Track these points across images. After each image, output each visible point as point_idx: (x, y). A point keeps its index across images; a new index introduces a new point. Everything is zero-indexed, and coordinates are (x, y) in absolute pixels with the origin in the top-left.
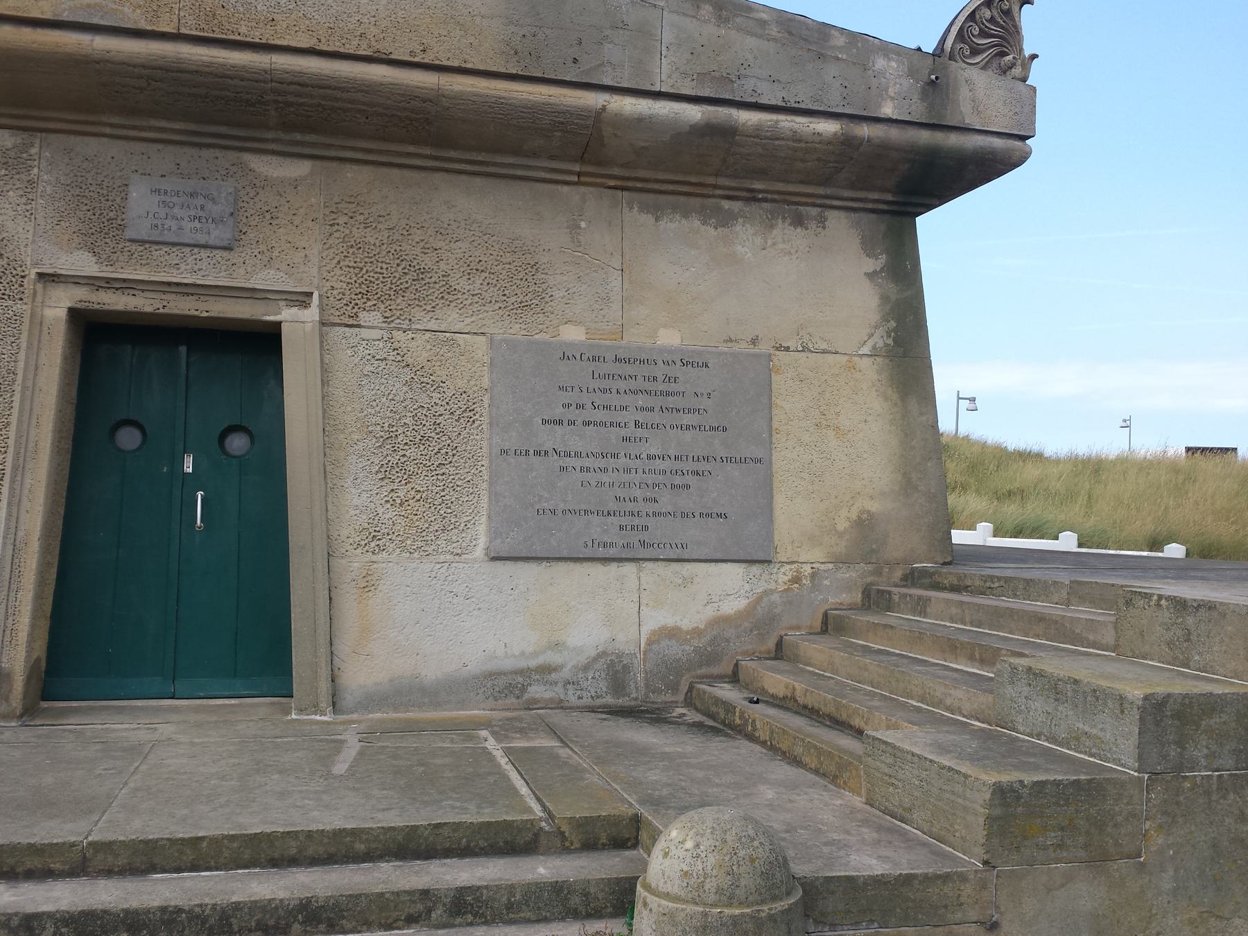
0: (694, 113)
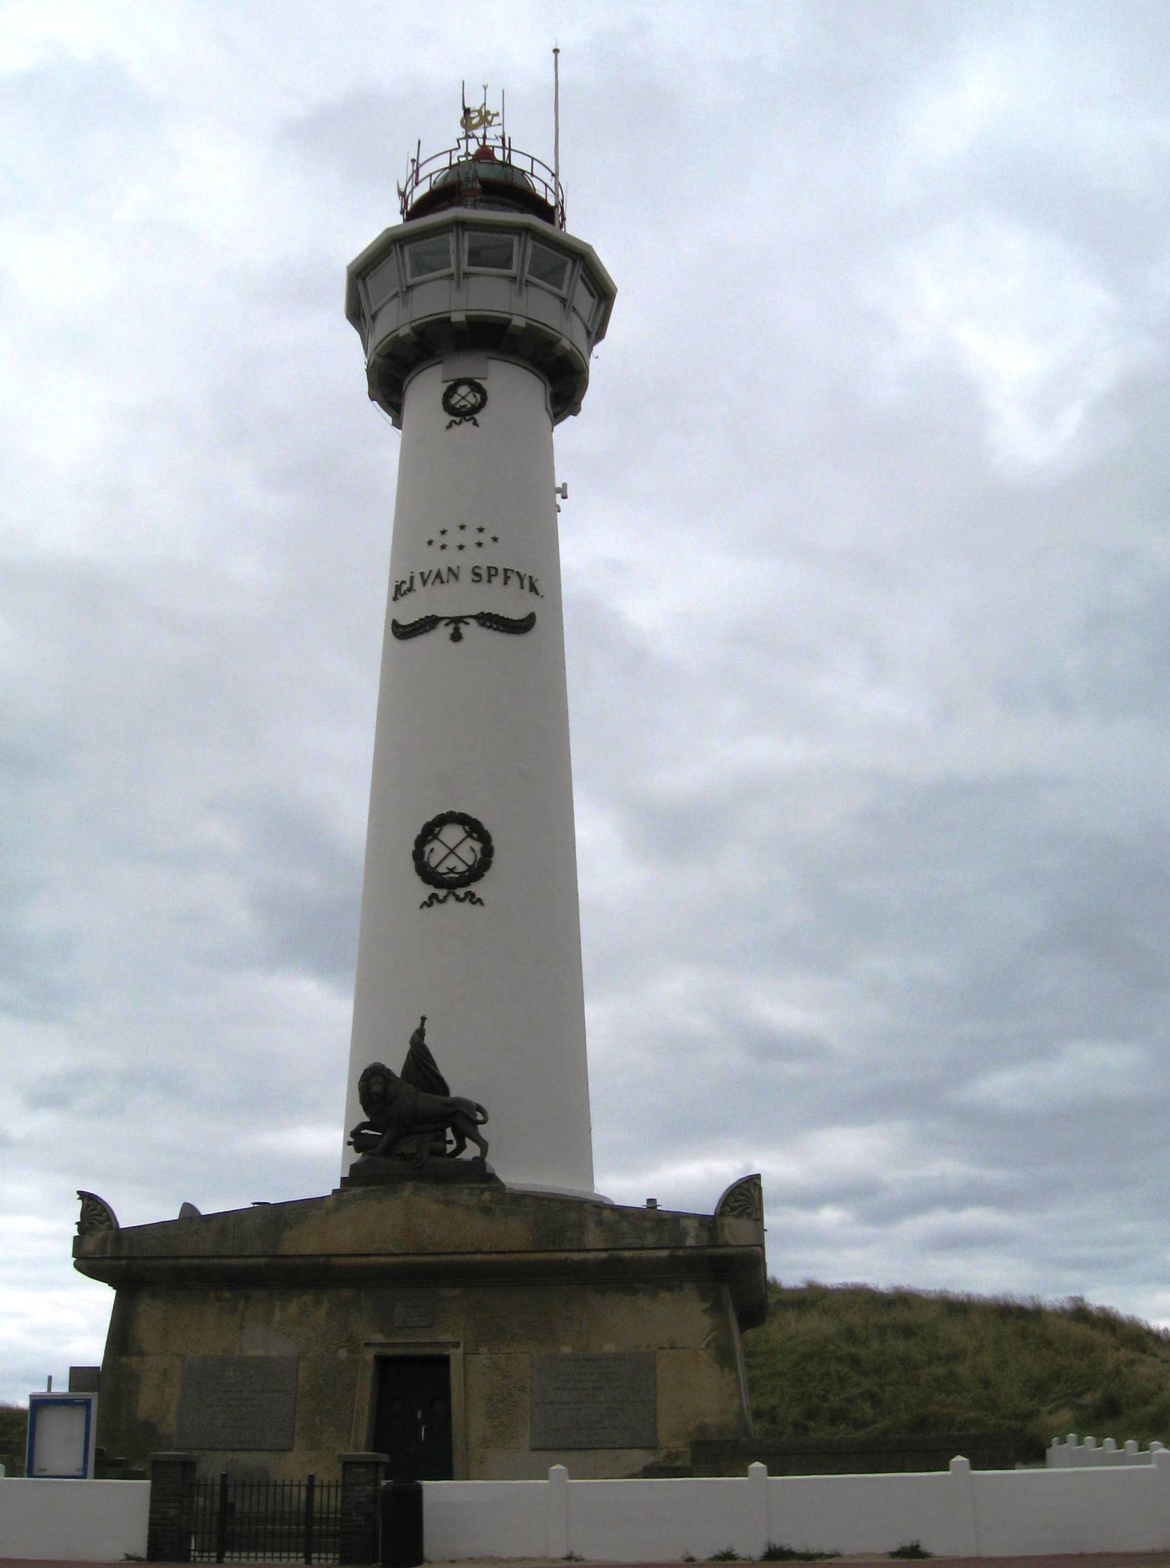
0: (604, 1255)
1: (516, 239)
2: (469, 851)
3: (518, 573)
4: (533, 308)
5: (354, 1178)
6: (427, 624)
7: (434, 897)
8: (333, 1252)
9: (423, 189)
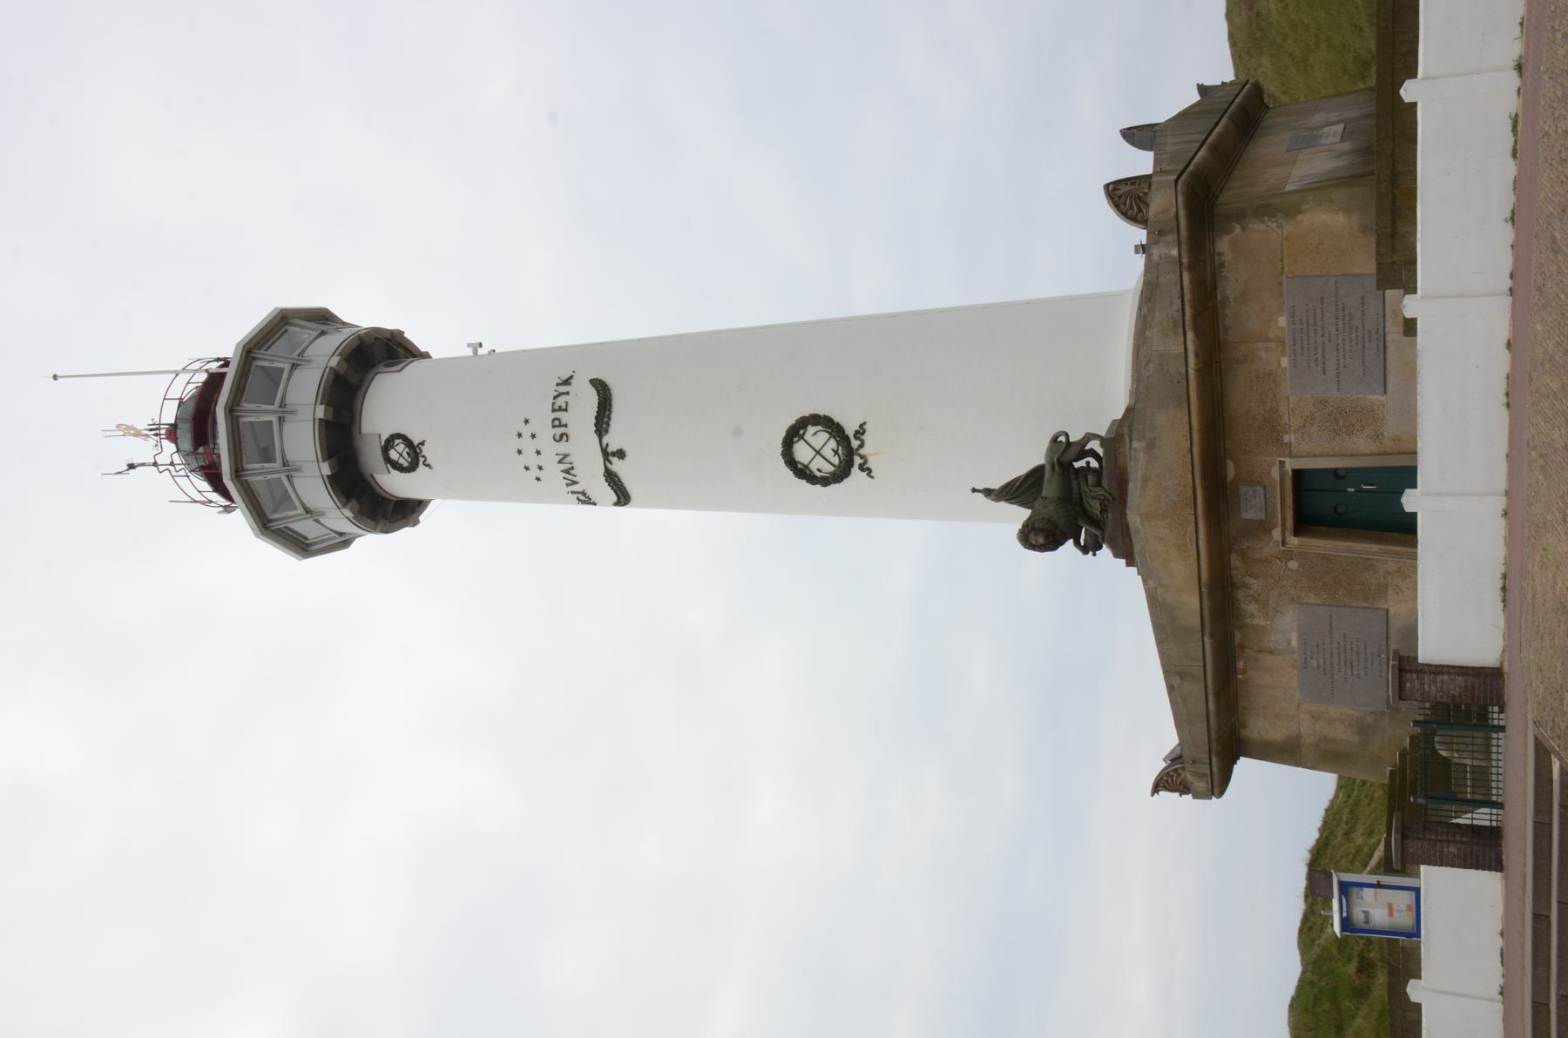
0: (1190, 335)
1: (242, 420)
2: (817, 437)
4: (304, 393)
5: (1126, 552)
6: (612, 479)
7: (862, 468)
9: (216, 497)
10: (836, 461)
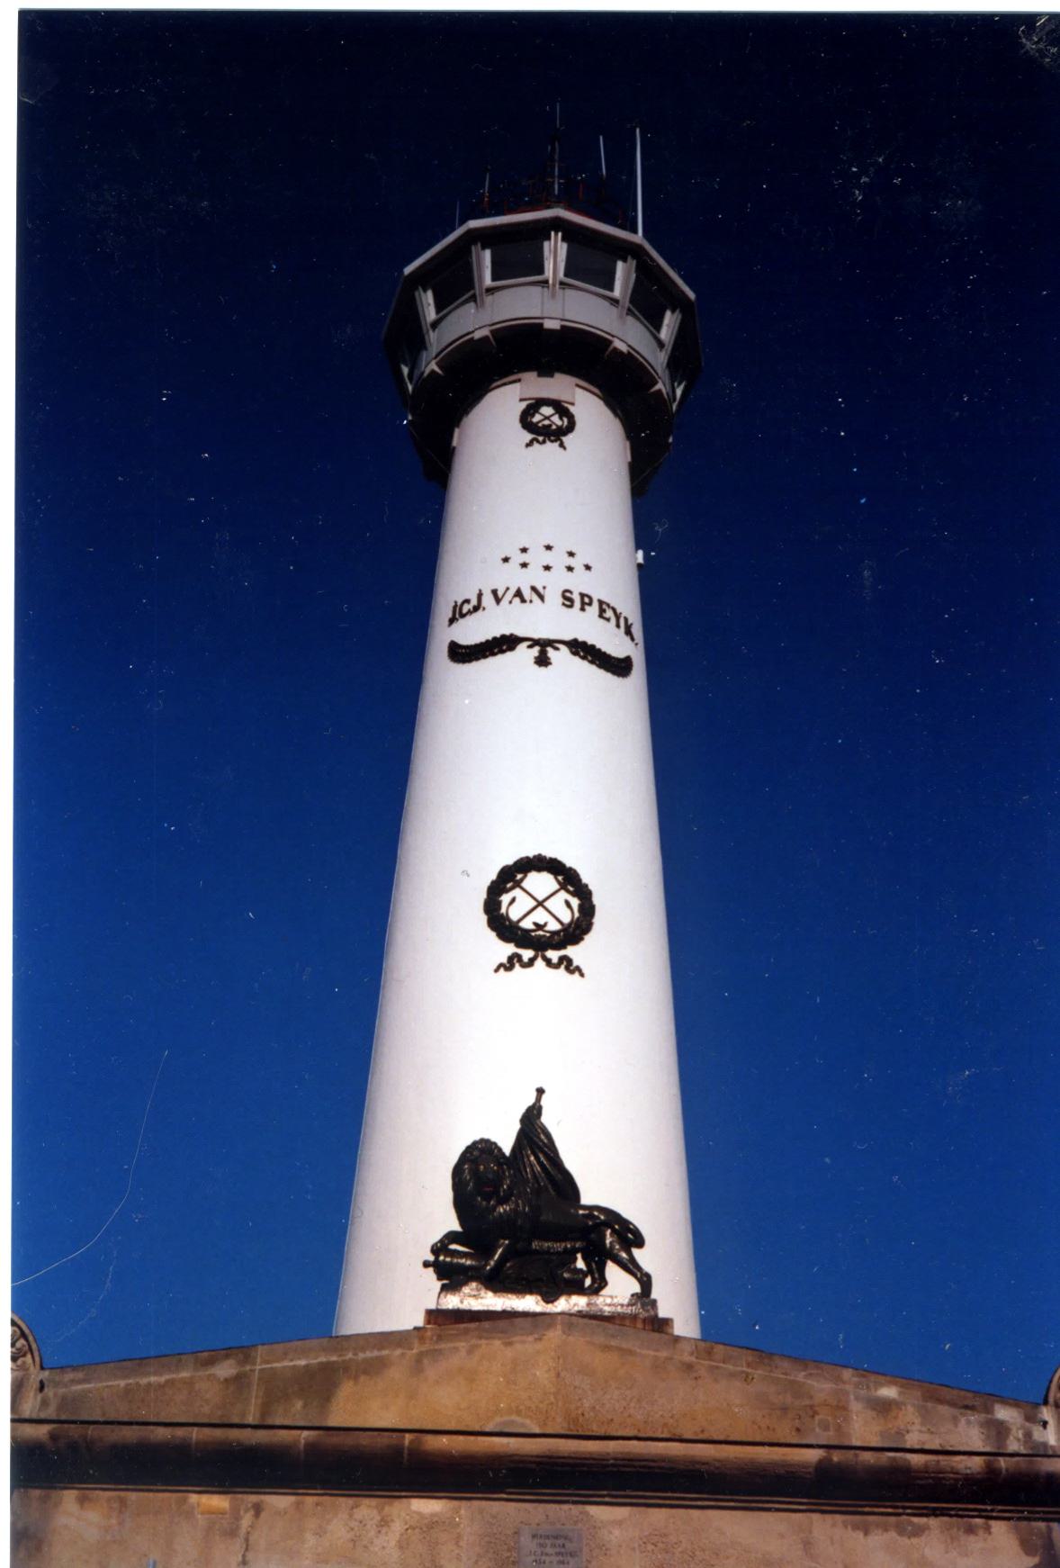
2: (562, 909)
3: (614, 610)
8: (430, 1427)
10: (527, 924)
